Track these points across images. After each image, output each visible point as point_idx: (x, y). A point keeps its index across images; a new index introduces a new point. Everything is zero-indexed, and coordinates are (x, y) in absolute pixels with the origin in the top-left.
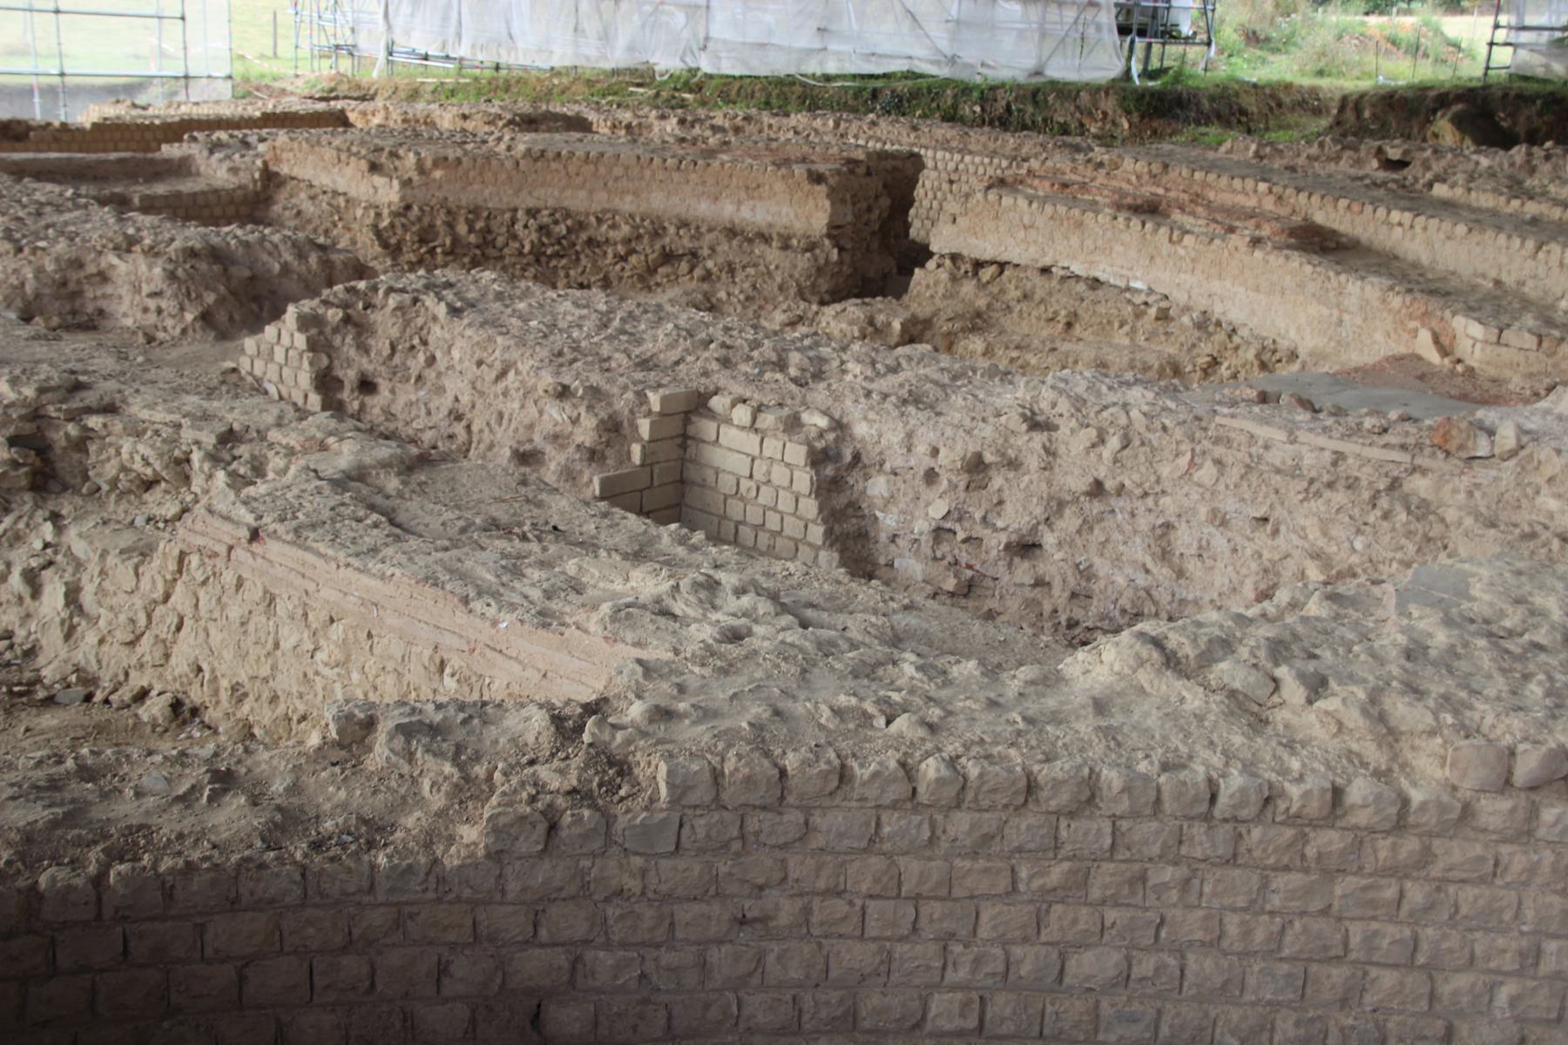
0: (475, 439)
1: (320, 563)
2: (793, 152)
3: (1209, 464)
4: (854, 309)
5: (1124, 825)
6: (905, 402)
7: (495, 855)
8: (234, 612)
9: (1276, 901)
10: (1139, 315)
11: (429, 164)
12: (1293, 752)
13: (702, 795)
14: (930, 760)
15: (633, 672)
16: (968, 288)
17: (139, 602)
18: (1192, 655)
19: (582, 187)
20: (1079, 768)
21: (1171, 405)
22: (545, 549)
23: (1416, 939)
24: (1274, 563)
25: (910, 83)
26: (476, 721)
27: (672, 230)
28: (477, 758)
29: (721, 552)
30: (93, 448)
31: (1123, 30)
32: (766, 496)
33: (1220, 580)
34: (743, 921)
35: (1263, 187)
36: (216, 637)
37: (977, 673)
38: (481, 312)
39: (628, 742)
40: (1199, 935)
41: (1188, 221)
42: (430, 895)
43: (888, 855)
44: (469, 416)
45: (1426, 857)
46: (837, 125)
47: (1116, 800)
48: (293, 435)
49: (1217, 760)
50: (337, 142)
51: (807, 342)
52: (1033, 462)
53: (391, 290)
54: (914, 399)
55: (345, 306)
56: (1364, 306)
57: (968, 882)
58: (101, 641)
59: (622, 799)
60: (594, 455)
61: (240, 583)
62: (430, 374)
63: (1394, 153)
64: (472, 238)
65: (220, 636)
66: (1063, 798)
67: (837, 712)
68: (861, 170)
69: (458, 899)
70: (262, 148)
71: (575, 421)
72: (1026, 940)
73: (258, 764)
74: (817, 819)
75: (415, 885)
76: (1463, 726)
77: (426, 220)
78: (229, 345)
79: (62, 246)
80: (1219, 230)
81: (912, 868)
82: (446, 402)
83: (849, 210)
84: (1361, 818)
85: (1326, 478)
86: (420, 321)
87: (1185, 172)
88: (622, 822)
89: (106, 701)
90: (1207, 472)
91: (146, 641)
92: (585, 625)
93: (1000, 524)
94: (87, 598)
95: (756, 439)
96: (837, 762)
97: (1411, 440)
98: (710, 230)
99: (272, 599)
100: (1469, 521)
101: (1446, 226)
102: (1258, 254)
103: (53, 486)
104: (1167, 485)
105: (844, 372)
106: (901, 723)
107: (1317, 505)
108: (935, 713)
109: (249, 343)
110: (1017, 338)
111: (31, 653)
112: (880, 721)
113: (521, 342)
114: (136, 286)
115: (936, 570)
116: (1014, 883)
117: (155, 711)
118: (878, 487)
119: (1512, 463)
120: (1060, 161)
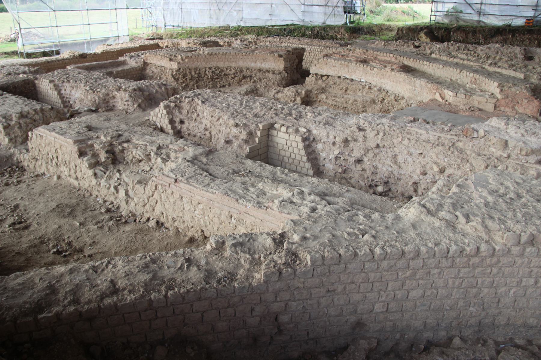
0: (213, 137)
1: (195, 189)
2: (274, 50)
3: (406, 140)
4: (292, 88)
5: (426, 260)
6: (325, 124)
7: (266, 282)
8: (172, 200)
9: (461, 275)
10: (363, 88)
11: (184, 58)
12: (466, 238)
13: (319, 262)
14: (377, 248)
15: (291, 224)
16: (320, 82)
17: (145, 197)
18: (434, 210)
19: (222, 61)
20: (415, 248)
21: (394, 123)
22: (250, 179)
23: (494, 281)
24: (424, 165)
25: (293, 26)
26: (251, 240)
27: (245, 71)
28: (254, 252)
29: (294, 175)
30: (125, 152)
31: (345, 12)
32: (291, 149)
33: (410, 169)
34: (328, 291)
35: (391, 55)
36: (167, 206)
37: (379, 217)
38: (210, 102)
39: (297, 248)
40: (442, 285)
41: (374, 64)
42: (249, 293)
43: (366, 273)
44: (210, 130)
45: (499, 261)
46: (280, 40)
47: (424, 255)
48: (176, 146)
49: (448, 241)
50: (161, 54)
51: (295, 107)
52: (361, 140)
53: (186, 97)
54: (327, 123)
55: (175, 102)
56: (421, 86)
57: (386, 277)
58: (136, 205)
59: (298, 265)
60: (246, 142)
61: (173, 193)
62: (198, 119)
63: (417, 44)
64: (196, 76)
65: (168, 206)
66: (412, 255)
67: (349, 234)
68: (291, 53)
69: (256, 293)
70: (142, 56)
71: (241, 133)
72: (399, 289)
73: (195, 255)
74: (348, 266)
75: (245, 291)
76: (506, 228)
77: (184, 72)
78: (145, 112)
79: (103, 90)
80: (383, 67)
81: (372, 275)
82: (203, 126)
83: (289, 63)
84: (484, 254)
85: (437, 143)
86: (194, 105)
87: (372, 52)
88: (298, 271)
89: (140, 221)
90: (406, 142)
91: (148, 206)
92: (272, 207)
93: (353, 155)
94: (131, 193)
95: (288, 135)
96: (353, 251)
97: (458, 133)
98: (255, 70)
99: (182, 197)
100: (473, 154)
101: (438, 65)
102: (393, 73)
103: (117, 162)
104: (396, 145)
105: (307, 115)
106: (366, 237)
107: (435, 150)
108: (373, 232)
109: (152, 113)
110: (333, 94)
111: (118, 208)
112: (361, 236)
113: (223, 111)
114: (122, 100)
115: (336, 167)
116: (397, 276)
117: (153, 224)
118: (320, 146)
119: (483, 139)
120: (340, 49)
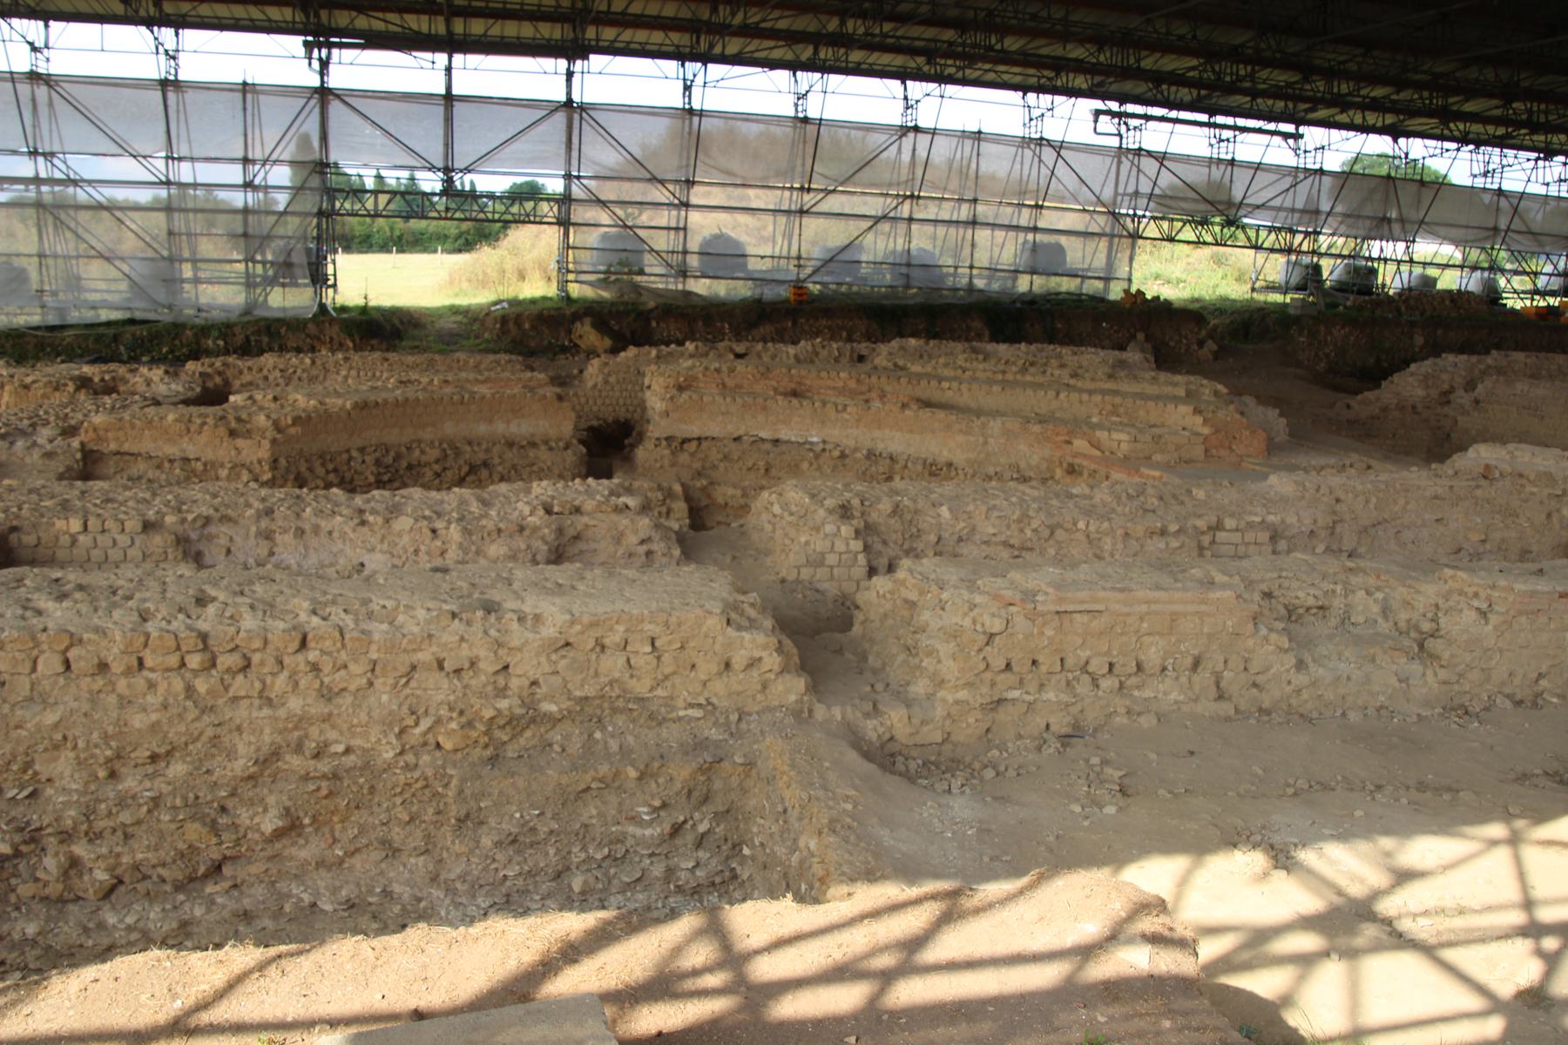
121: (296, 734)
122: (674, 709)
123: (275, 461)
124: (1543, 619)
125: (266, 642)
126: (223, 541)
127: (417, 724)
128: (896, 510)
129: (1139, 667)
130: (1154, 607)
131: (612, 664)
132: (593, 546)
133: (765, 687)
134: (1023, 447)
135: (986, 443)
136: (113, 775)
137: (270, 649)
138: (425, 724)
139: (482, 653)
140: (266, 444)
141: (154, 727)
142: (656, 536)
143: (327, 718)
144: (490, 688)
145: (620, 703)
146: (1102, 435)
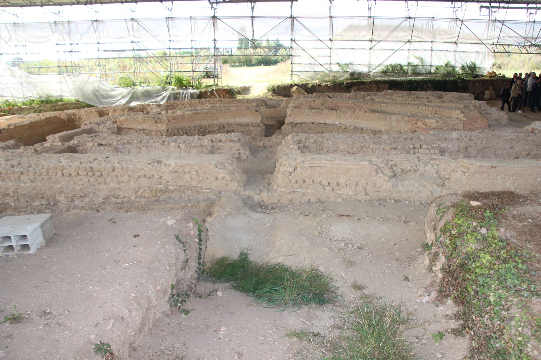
102: (367, 114)
121: (113, 192)
122: (202, 189)
123: (168, 130)
124: (485, 175)
125: (105, 169)
126: (128, 149)
127: (139, 191)
128: (315, 142)
129: (338, 184)
130: (341, 166)
131: (187, 177)
132: (223, 151)
133: (227, 185)
134: (402, 125)
135: (391, 124)
136: (72, 201)
137: (106, 171)
138: (141, 191)
139: (155, 173)
140: (165, 125)
141: (81, 189)
142: (241, 149)
143: (119, 189)
144: (157, 183)
145: (189, 188)
146: (427, 120)
